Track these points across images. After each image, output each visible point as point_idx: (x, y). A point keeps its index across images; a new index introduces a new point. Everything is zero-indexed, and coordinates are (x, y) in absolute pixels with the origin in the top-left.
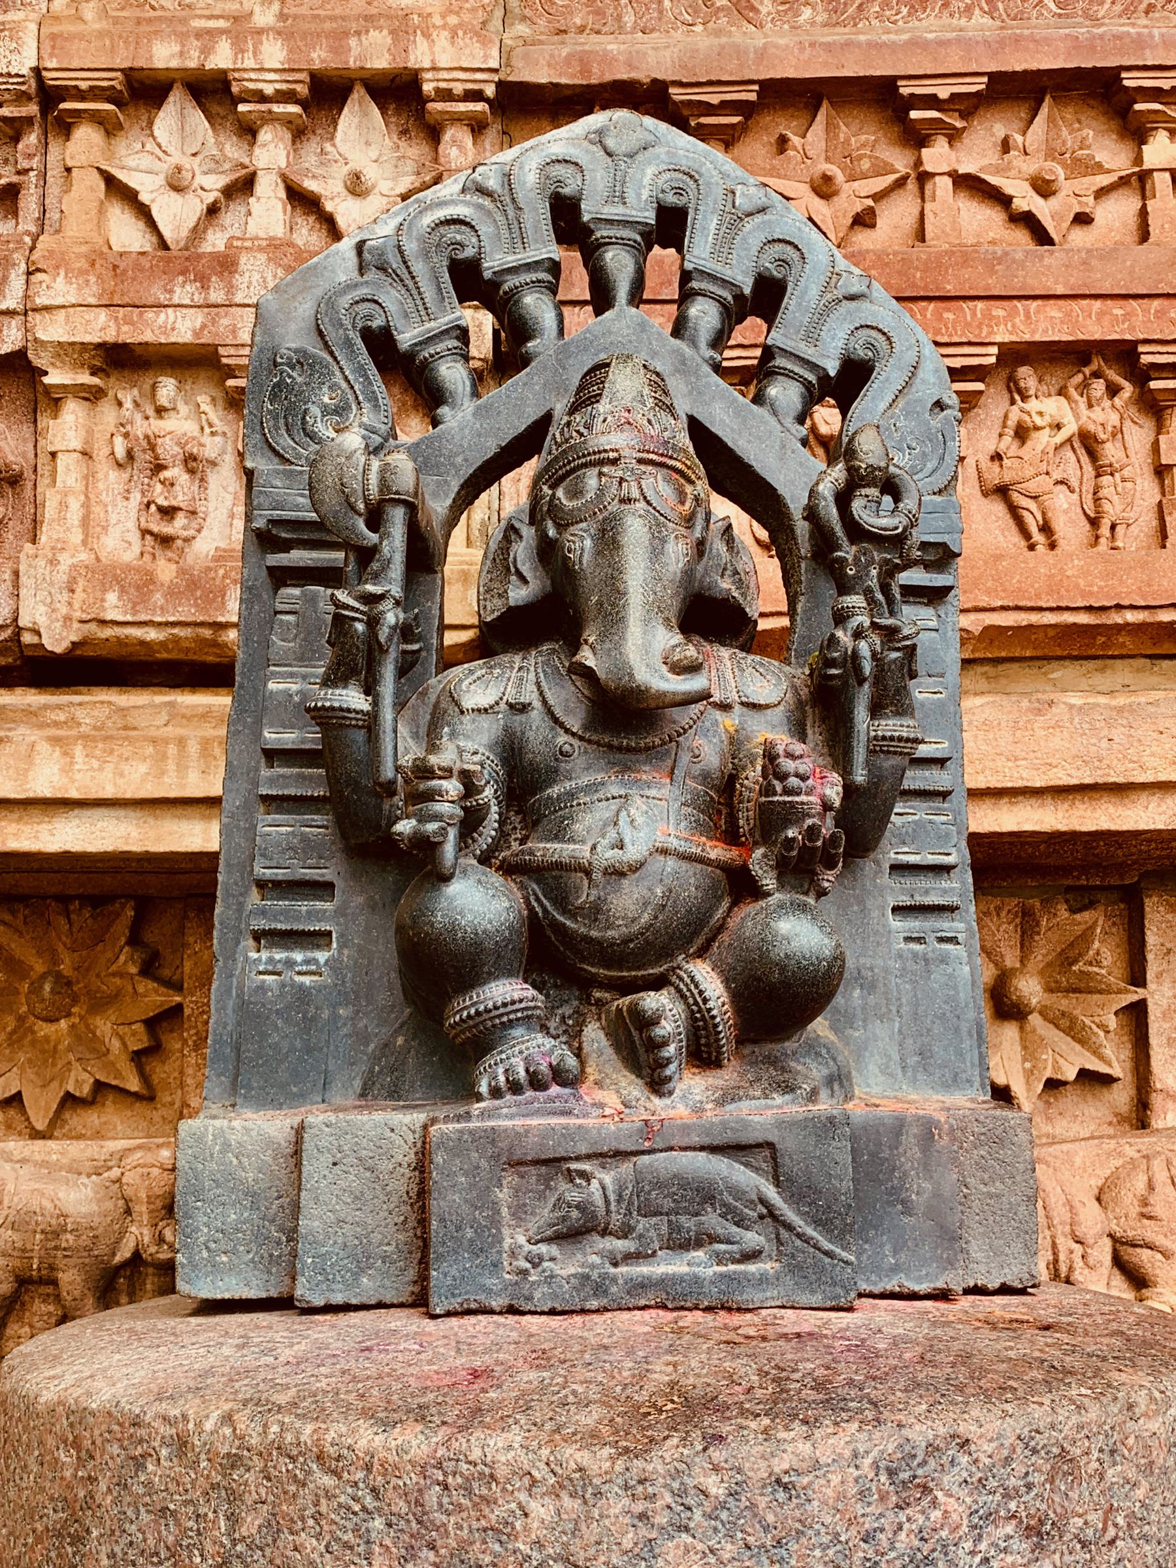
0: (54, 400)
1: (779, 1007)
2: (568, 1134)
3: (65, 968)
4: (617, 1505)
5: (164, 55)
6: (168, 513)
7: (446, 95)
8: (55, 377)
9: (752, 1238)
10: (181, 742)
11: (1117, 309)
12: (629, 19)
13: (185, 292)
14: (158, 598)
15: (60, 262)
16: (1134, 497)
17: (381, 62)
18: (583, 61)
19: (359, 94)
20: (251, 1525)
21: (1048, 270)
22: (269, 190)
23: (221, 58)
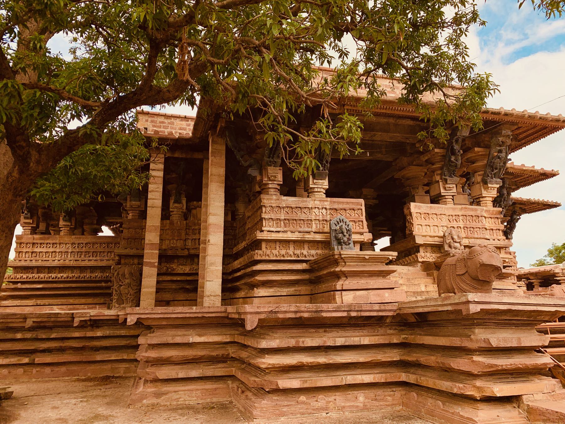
16: (354, 227)
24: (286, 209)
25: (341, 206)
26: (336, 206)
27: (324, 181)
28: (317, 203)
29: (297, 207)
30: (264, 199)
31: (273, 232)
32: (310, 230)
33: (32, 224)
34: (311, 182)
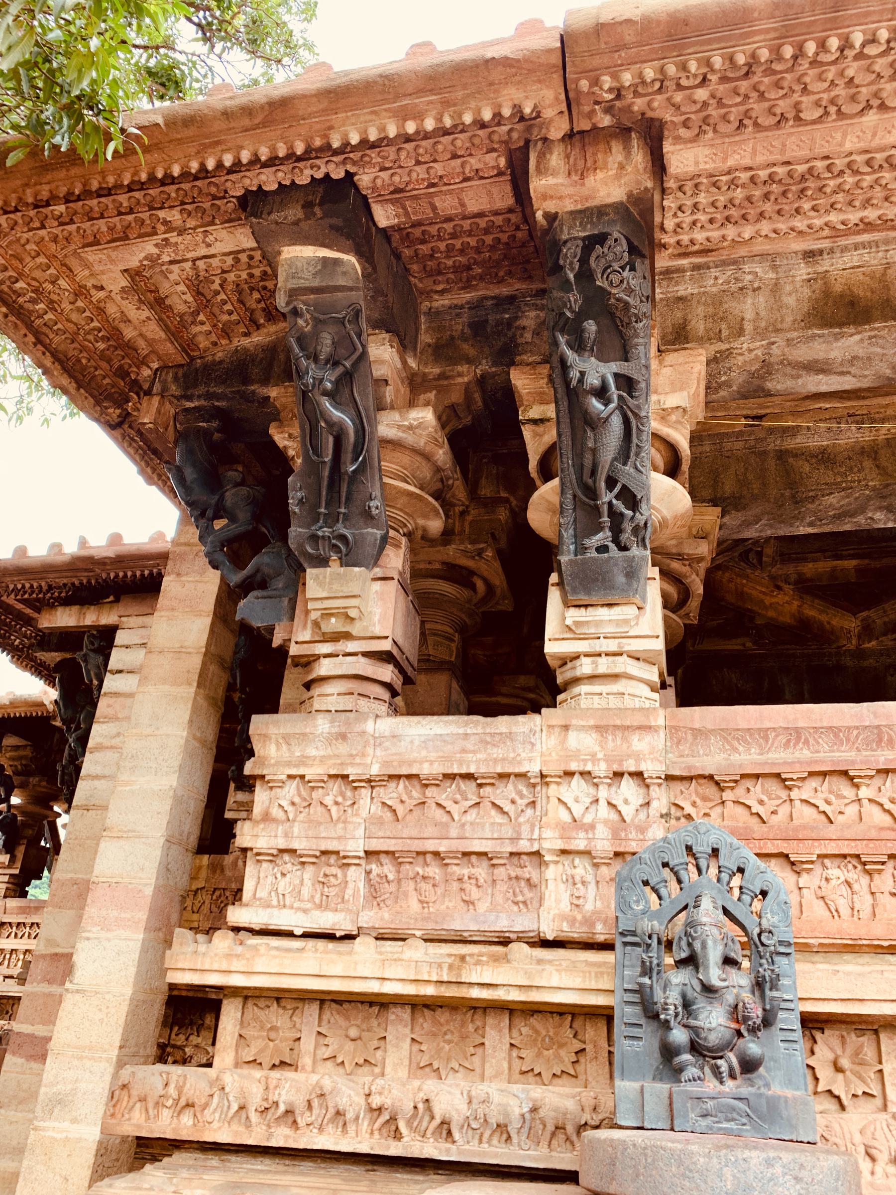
0: (547, 864)
1: (749, 1066)
2: (703, 1092)
3: (551, 1034)
4: (715, 1160)
5: (573, 766)
6: (578, 898)
7: (651, 778)
8: (547, 858)
9: (744, 1120)
10: (590, 973)
11: (853, 844)
12: (701, 752)
13: (582, 835)
14: (577, 925)
15: (548, 825)
16: (864, 902)
17: (632, 769)
18: (689, 768)
19: (626, 776)
20: (649, 1160)
21: (831, 831)
22: (603, 803)
23: (589, 768)
24: (392, 793)
25: (748, 758)
26: (711, 759)
27: (627, 611)
28: (583, 742)
29: (450, 777)
30: (265, 737)
31: (290, 934)
32: (522, 923)
33: (9, 866)
34: (551, 627)
